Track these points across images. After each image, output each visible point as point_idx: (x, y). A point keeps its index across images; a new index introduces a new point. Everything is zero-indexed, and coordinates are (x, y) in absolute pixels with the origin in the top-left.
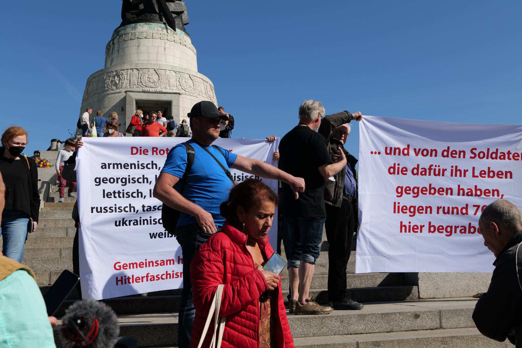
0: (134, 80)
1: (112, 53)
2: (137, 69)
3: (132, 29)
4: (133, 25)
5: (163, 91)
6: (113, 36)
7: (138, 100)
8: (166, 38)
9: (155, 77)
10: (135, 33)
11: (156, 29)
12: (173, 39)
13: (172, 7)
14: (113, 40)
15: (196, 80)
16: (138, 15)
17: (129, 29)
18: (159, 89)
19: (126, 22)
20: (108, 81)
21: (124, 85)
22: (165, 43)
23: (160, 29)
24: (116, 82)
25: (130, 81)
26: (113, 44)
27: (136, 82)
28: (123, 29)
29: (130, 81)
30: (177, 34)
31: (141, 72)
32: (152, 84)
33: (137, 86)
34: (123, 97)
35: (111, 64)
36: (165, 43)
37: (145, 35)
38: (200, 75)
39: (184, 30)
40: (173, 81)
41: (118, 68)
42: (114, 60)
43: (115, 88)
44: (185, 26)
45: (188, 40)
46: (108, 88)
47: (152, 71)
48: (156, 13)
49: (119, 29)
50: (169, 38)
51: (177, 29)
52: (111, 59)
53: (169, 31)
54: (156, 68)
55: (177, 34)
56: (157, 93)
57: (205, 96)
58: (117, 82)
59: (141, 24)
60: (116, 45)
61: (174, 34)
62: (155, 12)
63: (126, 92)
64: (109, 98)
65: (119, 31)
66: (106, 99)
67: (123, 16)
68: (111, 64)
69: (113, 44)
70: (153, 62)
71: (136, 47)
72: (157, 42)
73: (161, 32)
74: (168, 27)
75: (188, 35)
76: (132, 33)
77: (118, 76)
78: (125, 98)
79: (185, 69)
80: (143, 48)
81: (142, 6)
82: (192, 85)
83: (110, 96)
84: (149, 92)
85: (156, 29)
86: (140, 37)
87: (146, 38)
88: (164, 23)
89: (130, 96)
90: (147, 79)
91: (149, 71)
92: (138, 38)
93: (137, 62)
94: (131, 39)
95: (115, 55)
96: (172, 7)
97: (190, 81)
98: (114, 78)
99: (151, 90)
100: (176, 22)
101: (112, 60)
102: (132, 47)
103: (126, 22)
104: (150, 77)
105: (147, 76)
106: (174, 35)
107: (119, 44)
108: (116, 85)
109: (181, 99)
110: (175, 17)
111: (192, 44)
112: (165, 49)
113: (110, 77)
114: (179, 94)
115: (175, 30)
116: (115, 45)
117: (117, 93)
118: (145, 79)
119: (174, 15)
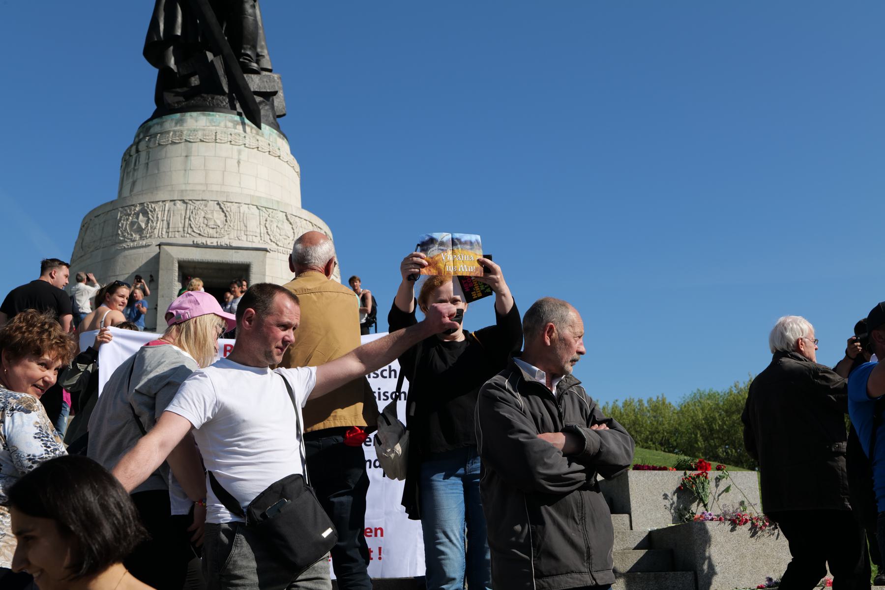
0: (177, 221)
1: (134, 170)
2: (183, 201)
3: (176, 124)
4: (178, 115)
5: (234, 245)
6: (138, 135)
7: (184, 262)
8: (241, 142)
9: (219, 217)
10: (182, 132)
11: (222, 124)
12: (254, 144)
13: (255, 83)
14: (137, 143)
15: (299, 224)
16: (188, 96)
17: (170, 123)
18: (225, 241)
19: (163, 109)
20: (125, 224)
21: (156, 232)
22: (239, 152)
23: (230, 124)
24: (140, 227)
25: (168, 224)
26: (137, 151)
27: (181, 226)
28: (157, 124)
29: (168, 224)
30: (262, 135)
31: (191, 207)
32: (211, 231)
33: (182, 233)
34: (153, 255)
35: (131, 191)
36: (239, 152)
37: (200, 135)
38: (306, 214)
39: (277, 127)
40: (253, 225)
41: (145, 199)
43: (137, 237)
44: (278, 120)
45: (283, 146)
46: (124, 236)
47: (212, 205)
48: (222, 93)
49: (150, 123)
50: (247, 141)
51: (263, 125)
52: (131, 180)
53: (248, 129)
54: (221, 199)
55: (262, 135)
58: (143, 226)
59: (194, 114)
60: (143, 155)
61: (258, 134)
62: (222, 93)
63: (159, 245)
64: (125, 257)
65: (150, 128)
66: (120, 259)
67: (159, 99)
68: (131, 191)
69: (137, 151)
70: (215, 188)
72: (225, 149)
73: (233, 131)
74: (247, 121)
75: (285, 136)
76: (175, 132)
77: (145, 213)
78: (156, 259)
79: (278, 202)
80: (195, 161)
81: (195, 81)
83: (127, 253)
85: (222, 124)
86: (191, 139)
87: (201, 141)
88: (239, 114)
89: (168, 254)
90: (201, 220)
91: (206, 206)
92: (186, 141)
93: (183, 187)
94: (173, 143)
95: (140, 173)
96: (255, 83)
98: (137, 218)
99: (209, 242)
100: (262, 112)
101: (134, 183)
102: (174, 157)
103: (163, 109)
104: (210, 216)
105: (203, 214)
106: (258, 137)
107: (148, 153)
108: (140, 230)
109: (268, 261)
110: (261, 103)
111: (292, 153)
112: (239, 162)
113: (129, 215)
114: (266, 250)
115: (259, 127)
116: (141, 154)
117: (142, 247)
119: (258, 99)
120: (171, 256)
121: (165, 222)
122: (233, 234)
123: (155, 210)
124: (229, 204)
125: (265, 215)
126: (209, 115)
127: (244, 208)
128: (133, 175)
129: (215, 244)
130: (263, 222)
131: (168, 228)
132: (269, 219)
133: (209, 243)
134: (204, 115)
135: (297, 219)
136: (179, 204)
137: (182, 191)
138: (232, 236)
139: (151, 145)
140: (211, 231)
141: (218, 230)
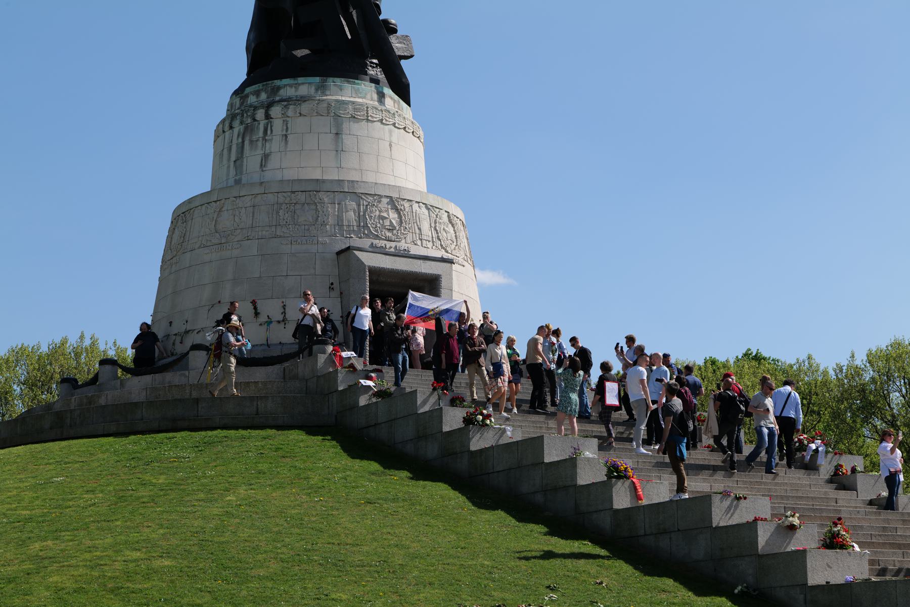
0: (351, 216)
4: (317, 79)
5: (414, 250)
8: (392, 121)
9: (393, 216)
18: (403, 245)
26: (268, 116)
28: (291, 86)
32: (389, 234)
40: (425, 226)
42: (272, 157)
52: (260, 152)
54: (395, 195)
56: (399, 254)
59: (338, 81)
60: (278, 124)
65: (279, 88)
69: (268, 116)
71: (331, 136)
84: (399, 254)
85: (369, 96)
89: (358, 260)
91: (380, 202)
95: (275, 145)
101: (266, 157)
104: (385, 215)
107: (286, 123)
109: (454, 273)
112: (390, 145)
114: (451, 262)
120: (363, 263)
126: (354, 83)
127: (415, 206)
128: (264, 146)
129: (392, 250)
130: (433, 225)
134: (349, 82)
137: (353, 181)
138: (409, 239)
139: (290, 112)
140: (389, 234)
141: (395, 232)
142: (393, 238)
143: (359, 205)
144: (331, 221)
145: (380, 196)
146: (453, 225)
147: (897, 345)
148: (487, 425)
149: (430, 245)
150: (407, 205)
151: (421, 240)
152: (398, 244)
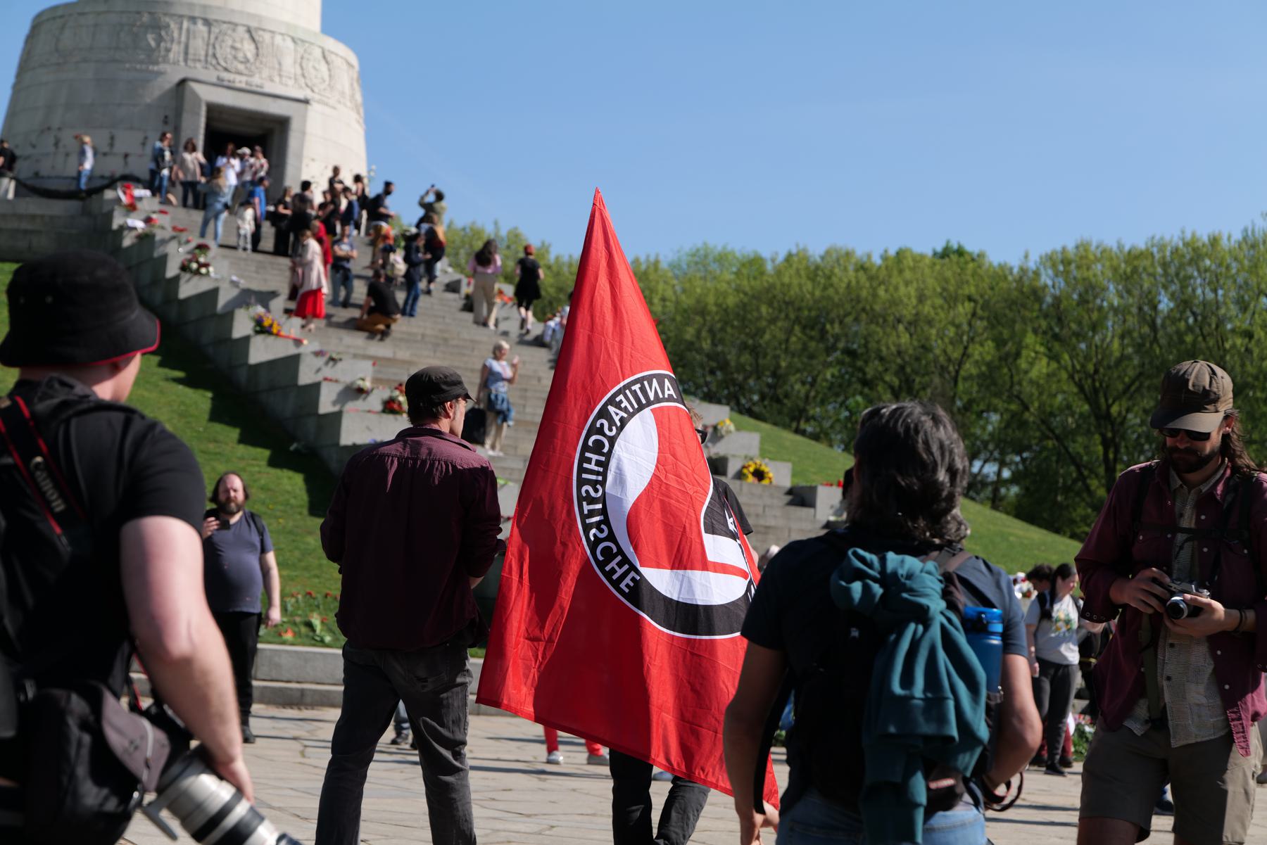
0: (198, 46)
2: (207, 22)
5: (268, 88)
9: (248, 48)
18: (256, 80)
21: (171, 55)
27: (203, 53)
31: (215, 30)
32: (241, 67)
47: (241, 30)
54: (253, 24)
57: (348, 104)
58: (153, 44)
82: (327, 78)
90: (228, 50)
91: (234, 30)
97: (323, 67)
99: (240, 81)
104: (238, 45)
105: (230, 42)
108: (150, 51)
114: (306, 102)
118: (224, 51)
121: (182, 46)
122: (266, 73)
123: (168, 26)
124: (261, 33)
125: (301, 50)
127: (278, 39)
129: (243, 86)
131: (186, 53)
132: (306, 56)
133: (238, 85)
135: (333, 57)
136: (201, 27)
140: (241, 67)
142: (245, 72)
143: (210, 32)
144: (175, 48)
145: (236, 25)
146: (327, 62)
147: (1083, 247)
148: (201, 274)
149: (291, 82)
150: (267, 36)
151: (280, 76)
152: (250, 79)
